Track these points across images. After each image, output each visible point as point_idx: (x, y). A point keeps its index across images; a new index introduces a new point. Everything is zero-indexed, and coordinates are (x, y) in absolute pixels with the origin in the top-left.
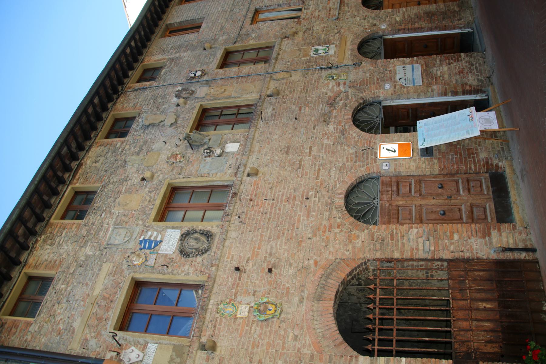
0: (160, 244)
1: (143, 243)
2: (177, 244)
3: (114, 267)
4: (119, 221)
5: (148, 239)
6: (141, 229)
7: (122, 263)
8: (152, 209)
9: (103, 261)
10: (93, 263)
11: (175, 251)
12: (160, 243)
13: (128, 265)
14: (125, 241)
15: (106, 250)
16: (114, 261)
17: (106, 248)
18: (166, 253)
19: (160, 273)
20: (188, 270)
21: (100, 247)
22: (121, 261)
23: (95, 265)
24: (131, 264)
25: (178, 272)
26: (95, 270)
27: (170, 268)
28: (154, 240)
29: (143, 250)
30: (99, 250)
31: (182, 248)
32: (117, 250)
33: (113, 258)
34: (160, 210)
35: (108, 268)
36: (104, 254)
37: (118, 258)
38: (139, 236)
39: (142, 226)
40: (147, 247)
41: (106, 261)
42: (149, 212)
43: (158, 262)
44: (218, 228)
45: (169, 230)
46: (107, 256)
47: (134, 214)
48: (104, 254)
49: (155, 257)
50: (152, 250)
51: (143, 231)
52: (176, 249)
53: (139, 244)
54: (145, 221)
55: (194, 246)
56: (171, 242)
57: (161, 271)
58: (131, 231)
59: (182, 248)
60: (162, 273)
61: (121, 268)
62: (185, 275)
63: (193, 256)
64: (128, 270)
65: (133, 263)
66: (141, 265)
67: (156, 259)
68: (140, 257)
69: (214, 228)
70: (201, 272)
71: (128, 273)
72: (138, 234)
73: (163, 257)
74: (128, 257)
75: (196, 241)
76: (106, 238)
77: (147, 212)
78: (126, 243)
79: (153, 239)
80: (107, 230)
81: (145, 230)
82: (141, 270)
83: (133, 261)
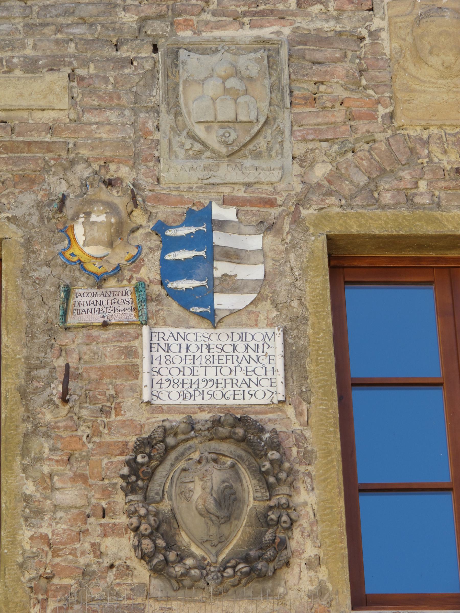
0: (193, 320)
1: (192, 230)
2: (201, 408)
3: (51, 129)
4: (319, 56)
5: (211, 247)
6: (281, 186)
7: (73, 163)
8: (410, 199)
9: (85, 64)
10: (69, 20)
11: (160, 409)
12: (200, 315)
13: (63, 200)
14: (200, 131)
15: (147, 51)
16: (88, 117)
17: (155, 49)
18: (146, 366)
19: (30, 368)
20: (56, 507)
21: (160, 17)
22: (84, 152)
23: (59, 30)
24: (69, 211)
25: (39, 459)
26: (30, 41)
27: (64, 410)
28: (211, 279)
29: (155, 241)
30: (143, 20)
31: (170, 441)
32: (148, 110)
33: (100, 108)
34: (420, 247)
35: (42, 103)
36: (124, 53)
37: (103, 133)
38: (240, 193)
39: (299, 188)
40: (170, 257)
41: (82, 79)
42: (387, 198)
43: (90, 340)
44: (312, 596)
45: (279, 340)
46: (112, 75)
47: (372, 117)
48: (124, 53)
49: (116, 318)
50: (156, 289)
51: (271, 203)
52: (171, 409)
53: (190, 212)
54: (329, 193)
55: (188, 499)
56: (211, 373)
57: (43, 373)
58: (261, 142)
59: (170, 441)
60: (30, 379)
61: (46, 169)
62: (27, 499)
63: (130, 515)
64: (39, 205)
65: (75, 218)
66: (67, 264)
67: (105, 324)
68: (111, 244)
69: (306, 574)
70: (49, 579)
71: (18, 212)
72: (248, 185)
73: (122, 361)
74: (109, 183)
75: (211, 505)
76: (219, 26)
77: (383, 185)
78: (188, 143)
79: (217, 274)
80: (263, 13)
81: (274, 212)
82: (44, 272)
83: (88, 214)
